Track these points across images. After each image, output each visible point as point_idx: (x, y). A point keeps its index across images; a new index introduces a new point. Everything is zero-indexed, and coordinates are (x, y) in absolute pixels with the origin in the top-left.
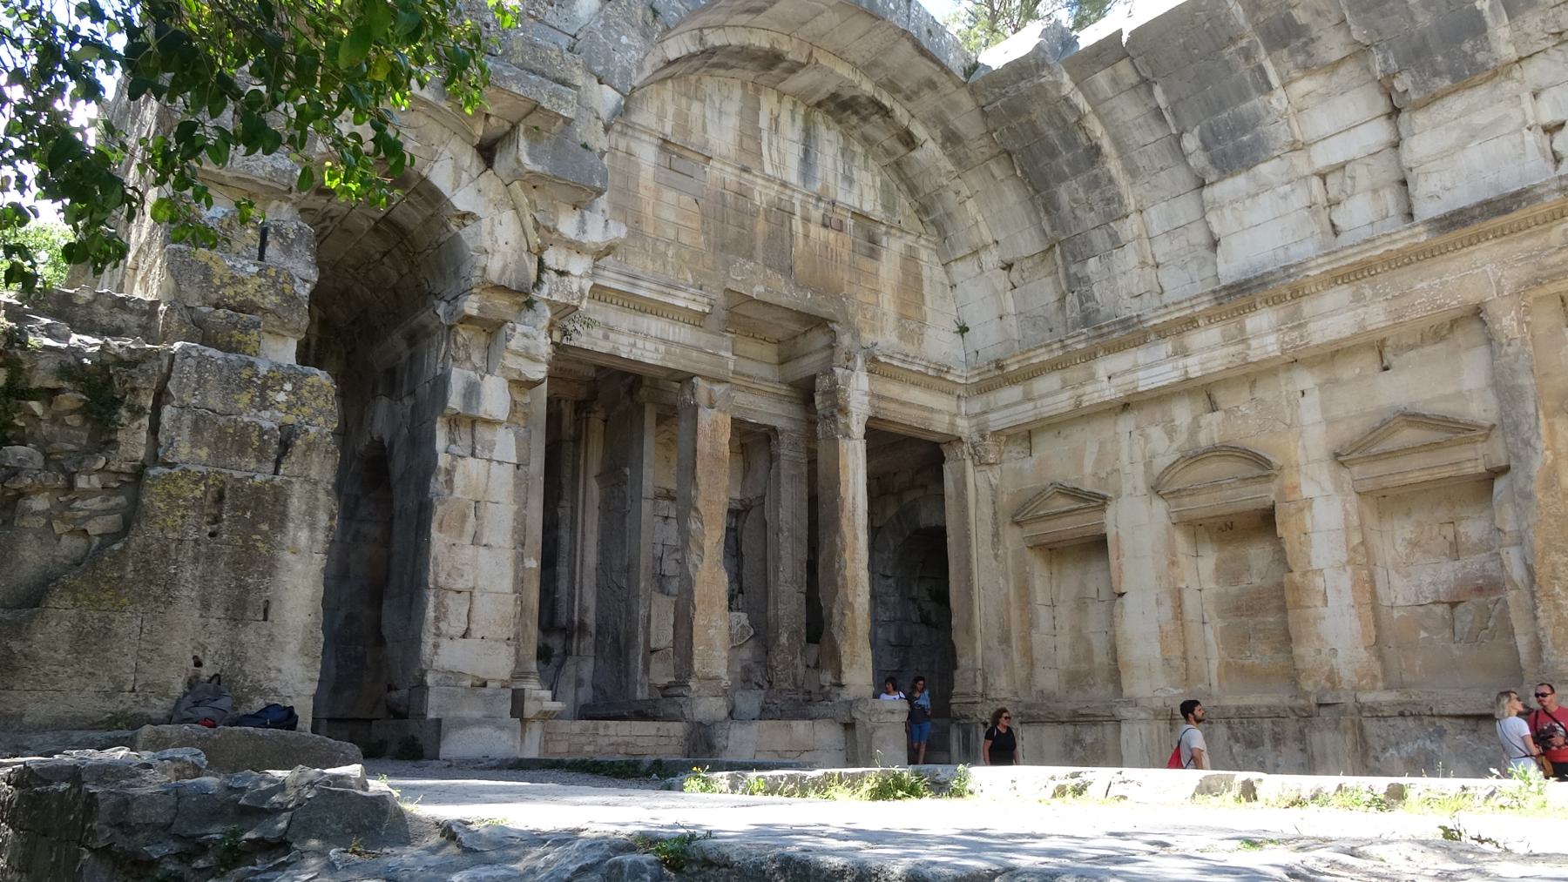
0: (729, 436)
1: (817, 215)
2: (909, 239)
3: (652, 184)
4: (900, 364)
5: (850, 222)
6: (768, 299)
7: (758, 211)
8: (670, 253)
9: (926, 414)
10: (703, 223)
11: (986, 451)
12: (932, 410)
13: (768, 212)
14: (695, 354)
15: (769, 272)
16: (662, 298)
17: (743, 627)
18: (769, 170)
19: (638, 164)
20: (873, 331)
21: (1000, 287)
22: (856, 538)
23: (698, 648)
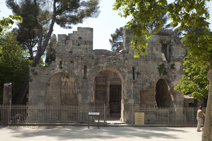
12: (118, 83)
20: (111, 77)
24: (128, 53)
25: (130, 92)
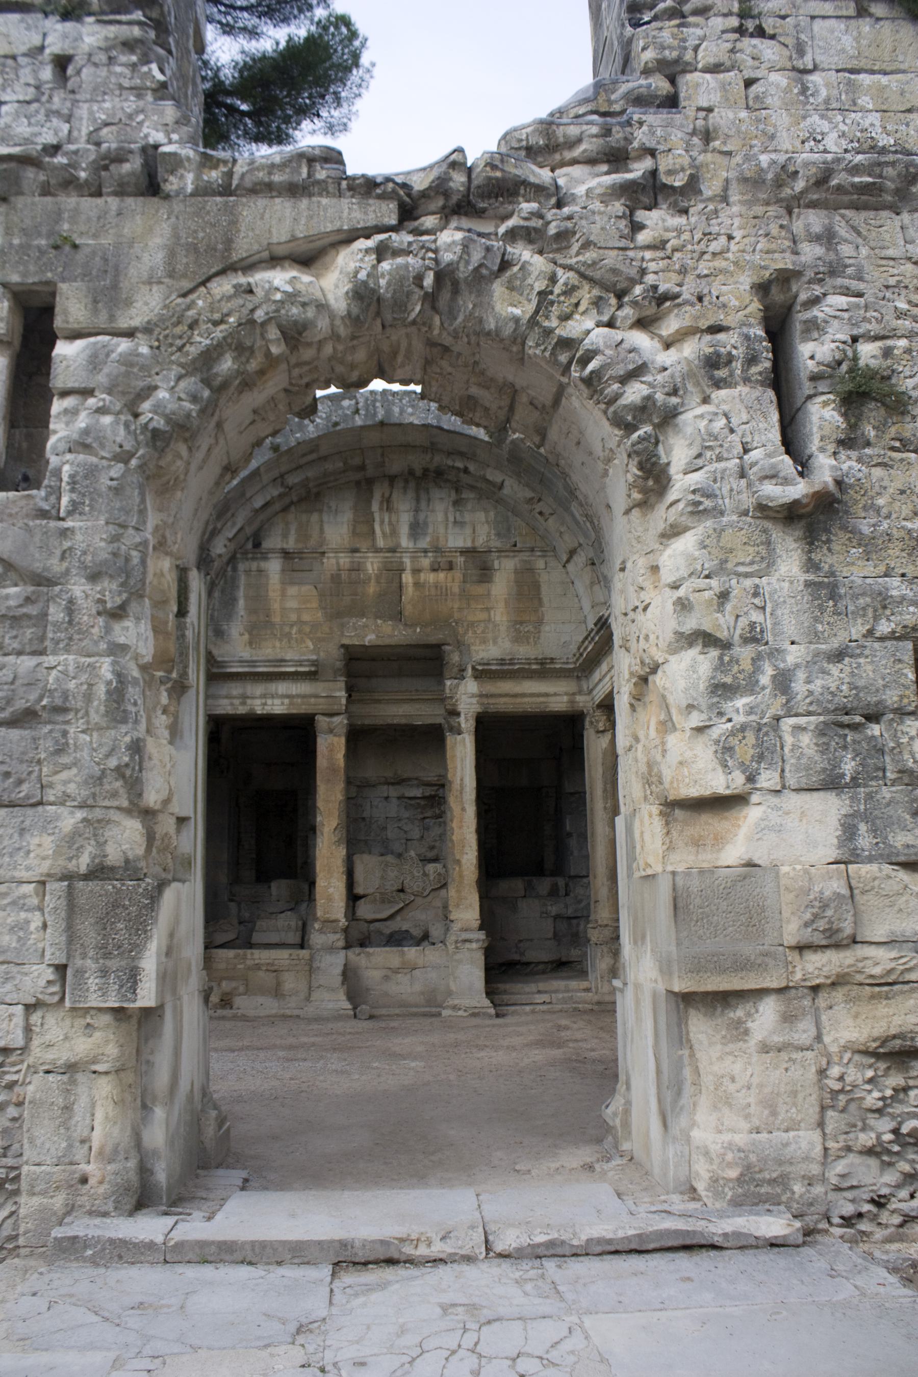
0: (343, 752)
1: (426, 562)
2: (525, 556)
3: (278, 587)
4: (498, 667)
5: (460, 560)
6: (380, 643)
7: (369, 579)
8: (294, 630)
9: (542, 699)
10: (321, 601)
11: (597, 721)
12: (547, 695)
13: (378, 578)
14: (313, 700)
15: (379, 622)
16: (276, 670)
17: (439, 874)
18: (381, 543)
19: (267, 577)
20: (484, 641)
21: (588, 582)
22: (463, 809)
23: (320, 901)
24: (672, 102)
25: (765, 679)
